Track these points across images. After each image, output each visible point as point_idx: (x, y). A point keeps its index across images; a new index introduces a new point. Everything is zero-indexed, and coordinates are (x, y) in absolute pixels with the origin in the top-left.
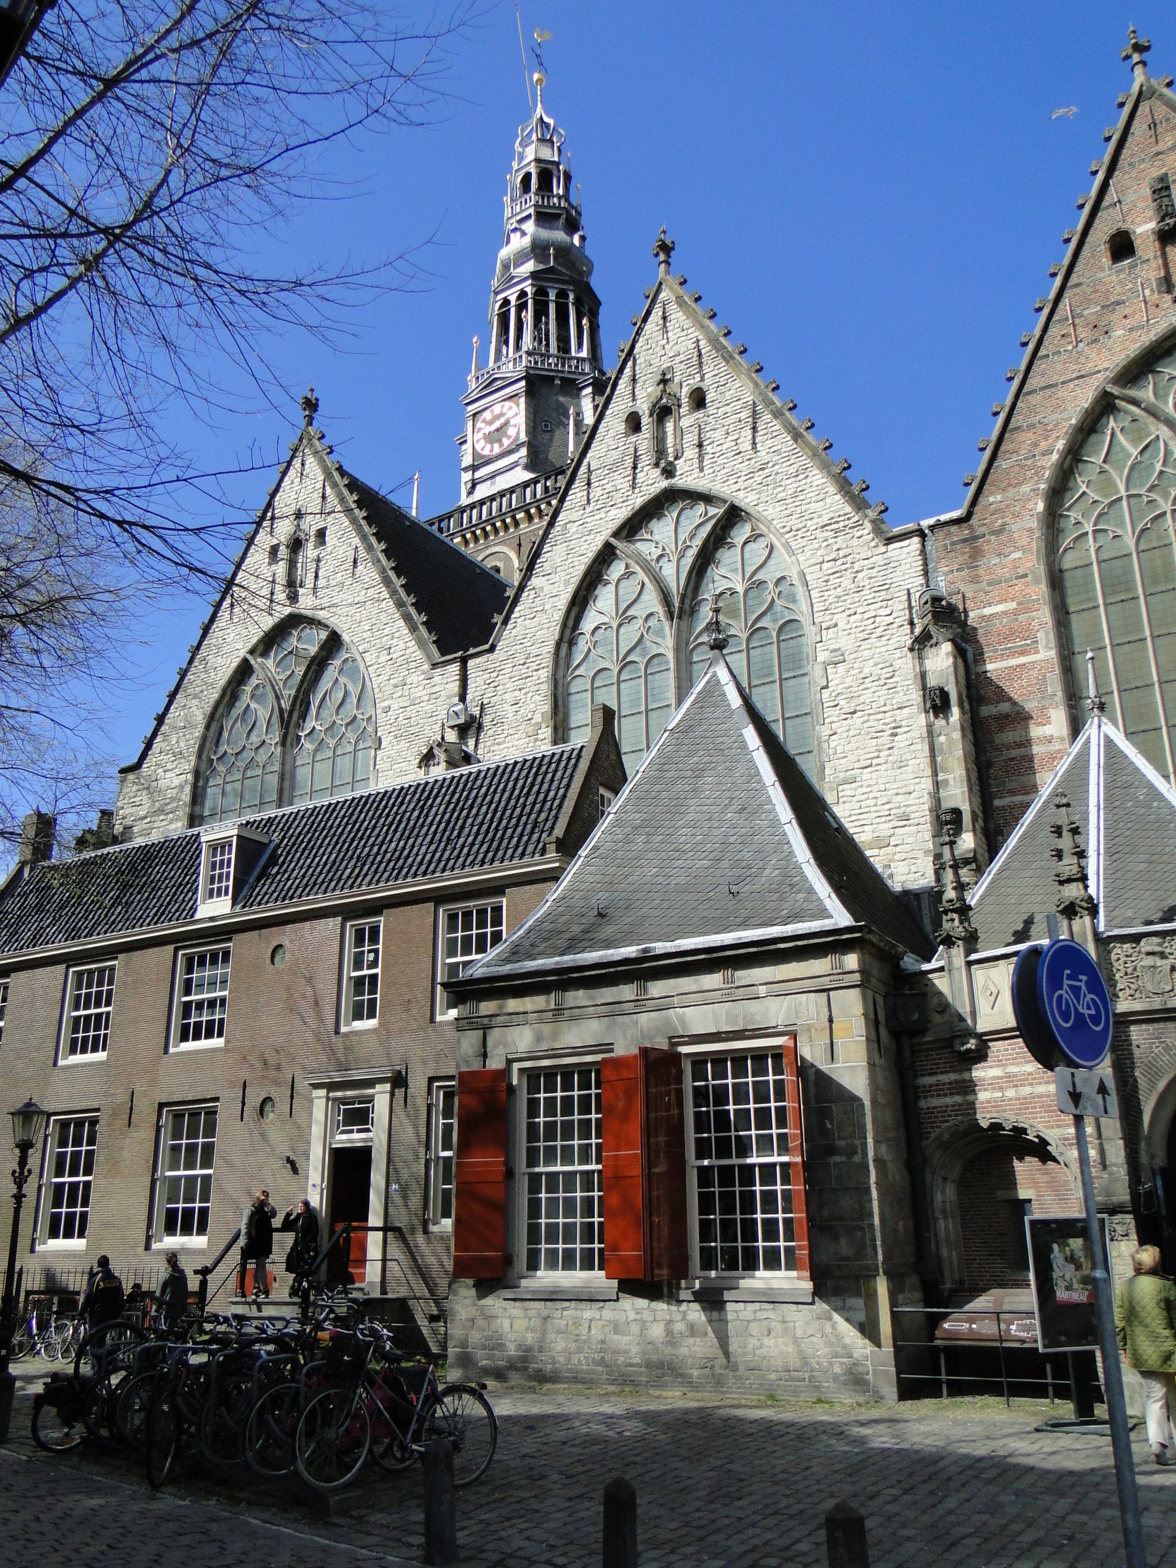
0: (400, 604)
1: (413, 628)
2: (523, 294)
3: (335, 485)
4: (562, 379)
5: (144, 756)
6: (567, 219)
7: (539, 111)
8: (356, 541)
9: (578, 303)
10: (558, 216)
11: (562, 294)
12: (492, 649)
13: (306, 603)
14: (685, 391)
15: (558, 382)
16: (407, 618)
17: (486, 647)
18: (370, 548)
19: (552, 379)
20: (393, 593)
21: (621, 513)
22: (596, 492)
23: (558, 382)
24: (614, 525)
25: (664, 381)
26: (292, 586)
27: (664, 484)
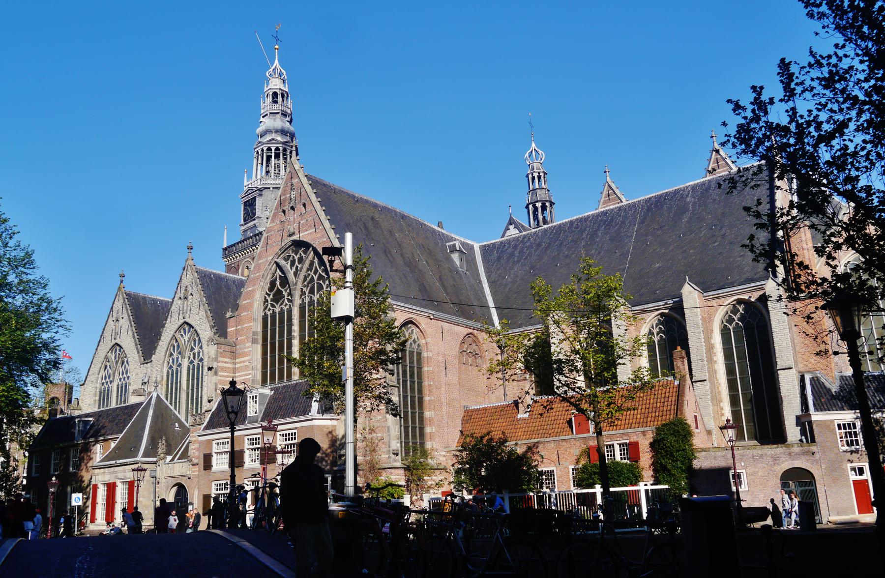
0: (136, 345)
1: (138, 352)
2: (262, 150)
3: (126, 304)
4: (273, 188)
5: (85, 381)
6: (282, 114)
7: (277, 62)
8: (129, 323)
9: (285, 150)
10: (278, 113)
11: (277, 149)
12: (151, 362)
13: (118, 341)
14: (189, 293)
15: (271, 189)
16: (137, 349)
17: (149, 361)
18: (131, 326)
19: (269, 188)
20: (135, 341)
21: (176, 327)
22: (173, 320)
23: (271, 189)
24: (175, 330)
25: (186, 290)
26: (116, 334)
27: (184, 320)
